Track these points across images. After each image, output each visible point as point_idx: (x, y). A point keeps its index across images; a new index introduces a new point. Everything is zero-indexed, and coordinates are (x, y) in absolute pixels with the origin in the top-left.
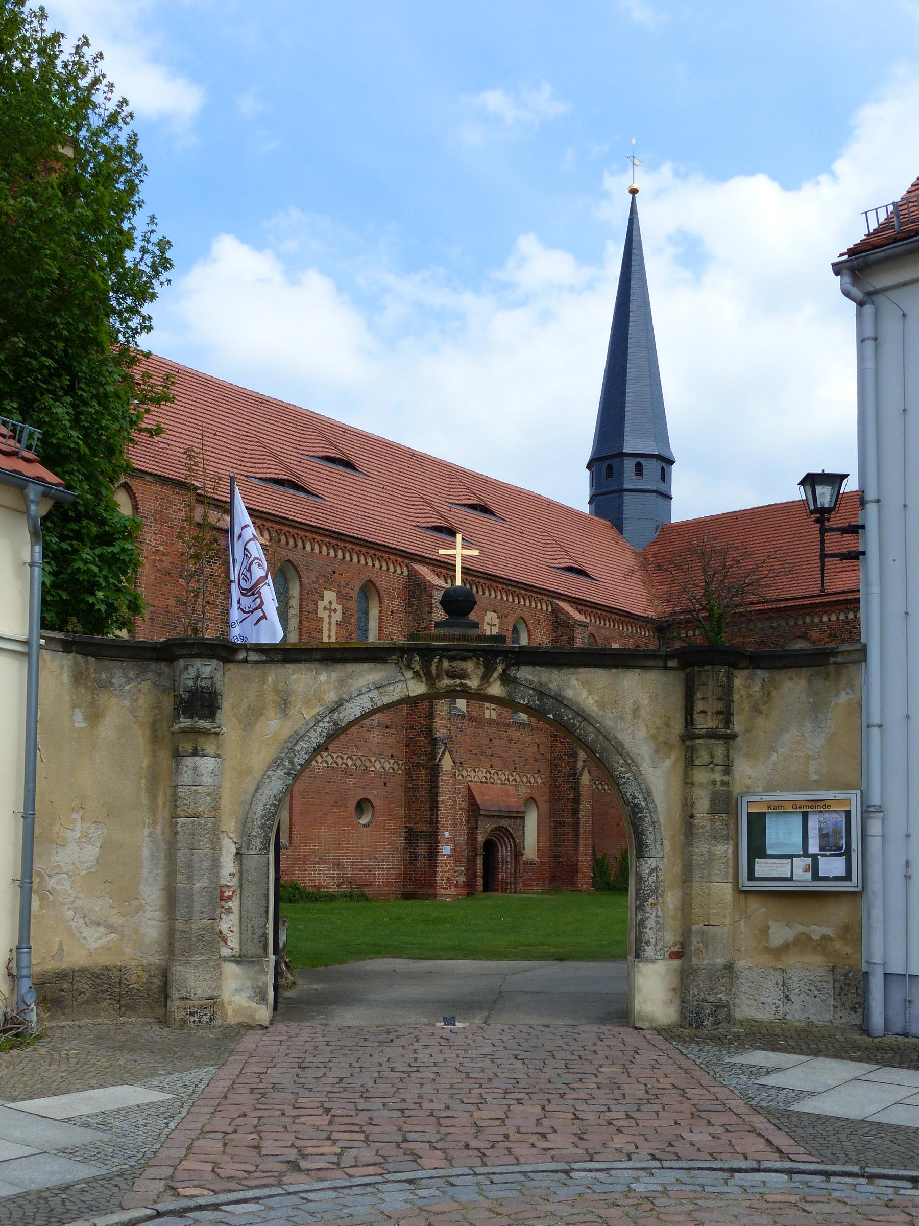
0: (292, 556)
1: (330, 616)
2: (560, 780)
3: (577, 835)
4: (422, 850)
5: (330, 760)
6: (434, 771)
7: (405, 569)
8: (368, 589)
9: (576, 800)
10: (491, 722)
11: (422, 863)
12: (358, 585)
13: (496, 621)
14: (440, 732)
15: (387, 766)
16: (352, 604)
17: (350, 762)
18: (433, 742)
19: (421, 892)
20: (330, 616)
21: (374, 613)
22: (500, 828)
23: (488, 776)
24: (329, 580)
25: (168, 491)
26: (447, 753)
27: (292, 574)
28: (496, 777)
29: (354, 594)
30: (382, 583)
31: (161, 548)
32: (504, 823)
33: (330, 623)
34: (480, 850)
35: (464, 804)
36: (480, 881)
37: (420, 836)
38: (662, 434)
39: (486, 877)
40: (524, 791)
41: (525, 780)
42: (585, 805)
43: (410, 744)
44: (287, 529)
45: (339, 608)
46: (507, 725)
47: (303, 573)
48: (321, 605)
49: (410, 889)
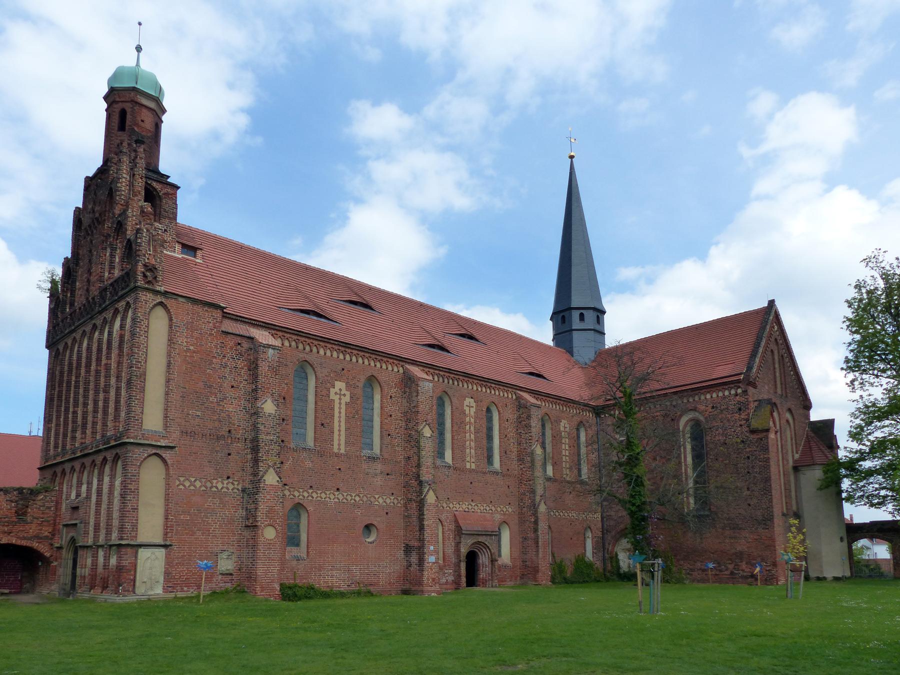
0: (308, 358)
1: (340, 399)
2: (525, 509)
3: (537, 547)
4: (414, 559)
5: (341, 497)
6: (421, 504)
7: (401, 369)
8: (372, 380)
9: (536, 523)
10: (471, 471)
11: (414, 568)
12: (363, 379)
13: (474, 404)
14: (425, 476)
15: (388, 501)
16: (359, 392)
17: (357, 499)
18: (421, 483)
19: (413, 588)
20: (340, 399)
21: (377, 397)
22: (479, 543)
23: (470, 507)
24: (340, 374)
25: (198, 309)
26: (431, 492)
27: (309, 370)
28: (476, 508)
29: (361, 385)
30: (382, 377)
31: (192, 348)
32: (481, 539)
33: (340, 403)
34: (463, 558)
35: (453, 527)
36: (464, 579)
37: (415, 549)
38: (596, 293)
39: (467, 577)
40: (498, 517)
41: (499, 509)
42: (543, 526)
43: (406, 486)
44: (303, 339)
45: (348, 393)
46: (485, 473)
47: (318, 369)
48: (332, 391)
49: (407, 586)
